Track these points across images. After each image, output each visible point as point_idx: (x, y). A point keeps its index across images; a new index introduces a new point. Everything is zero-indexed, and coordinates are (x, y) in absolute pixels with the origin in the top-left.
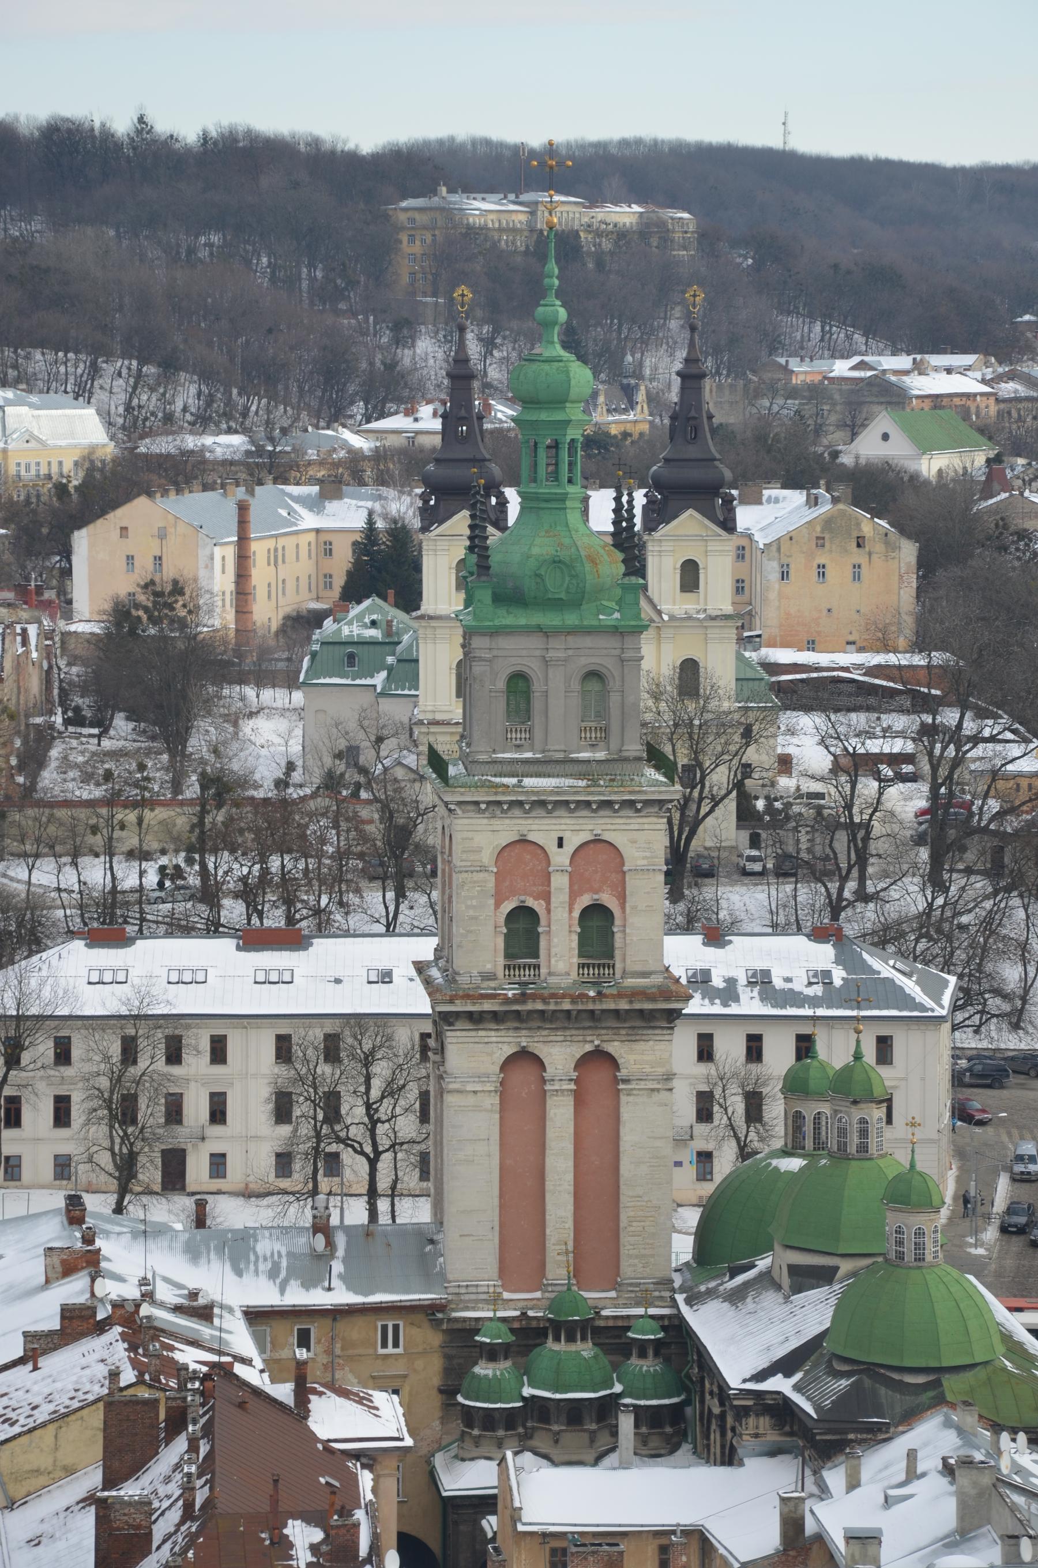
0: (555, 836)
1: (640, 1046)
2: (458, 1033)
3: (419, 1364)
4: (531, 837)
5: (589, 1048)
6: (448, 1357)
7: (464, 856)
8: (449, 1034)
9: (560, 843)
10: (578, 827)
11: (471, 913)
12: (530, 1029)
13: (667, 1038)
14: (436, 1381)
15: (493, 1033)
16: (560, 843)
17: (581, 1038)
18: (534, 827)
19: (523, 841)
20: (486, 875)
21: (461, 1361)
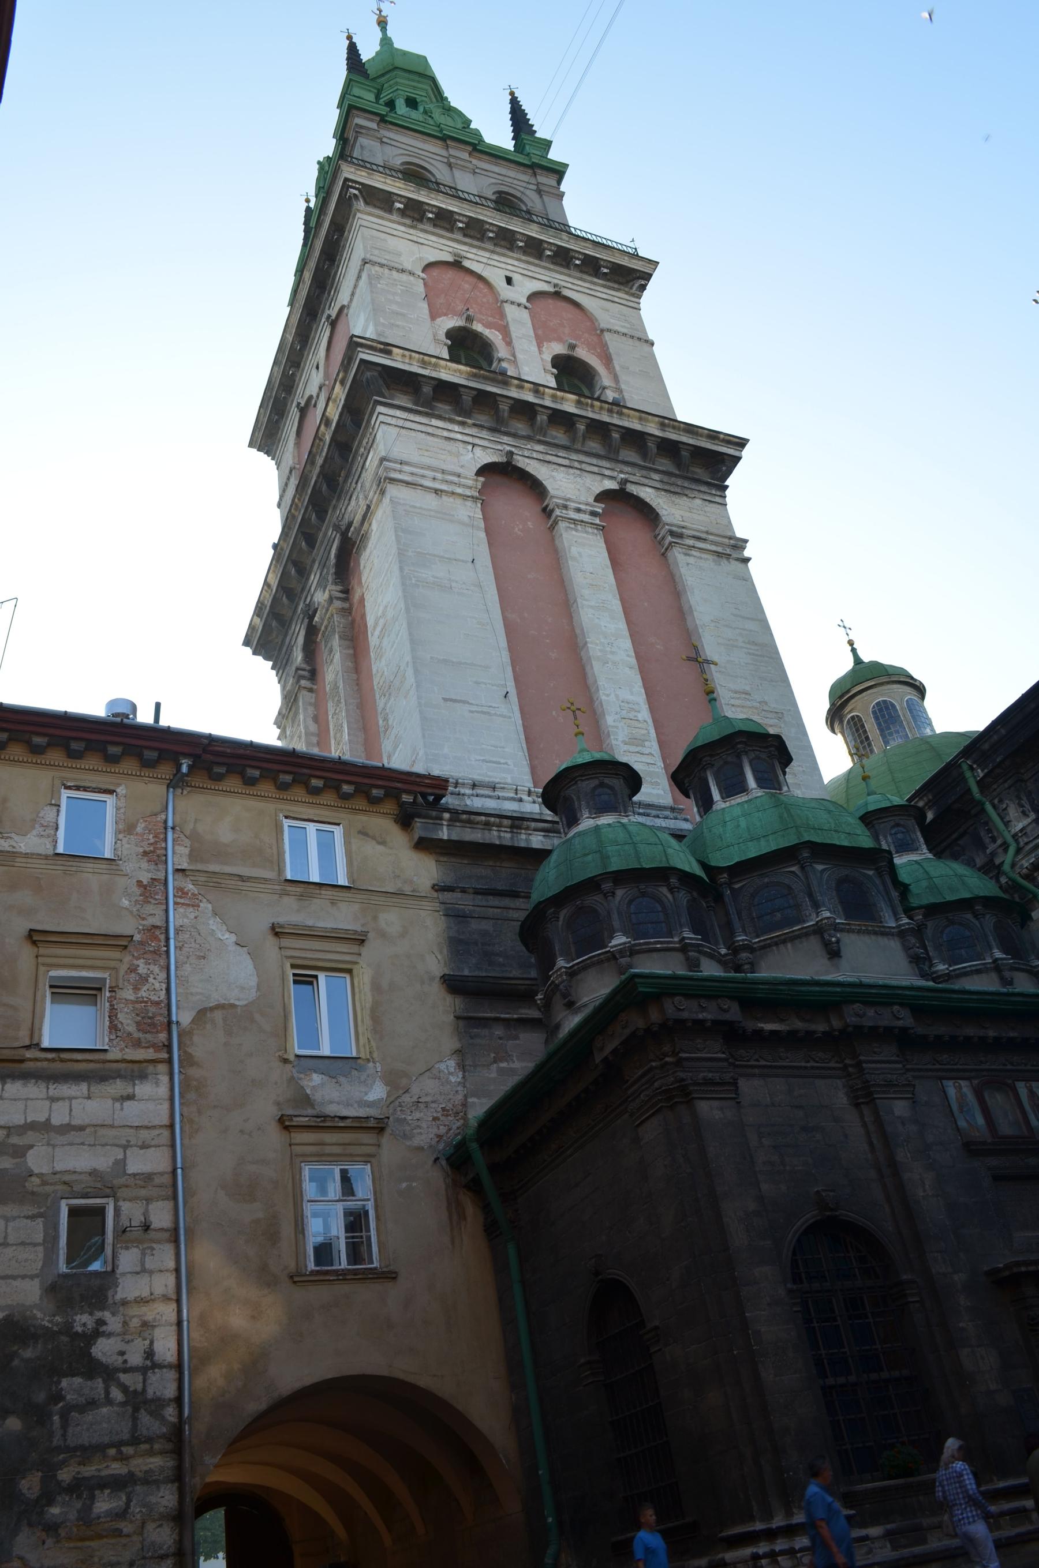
0: (503, 273)
1: (683, 501)
2: (398, 413)
3: (391, 919)
4: (466, 264)
5: (611, 485)
6: (455, 916)
7: (376, 252)
8: (380, 409)
9: (509, 281)
10: (530, 274)
11: (394, 307)
12: (514, 435)
13: (718, 499)
14: (436, 965)
15: (456, 428)
16: (509, 281)
17: (596, 469)
18: (469, 255)
19: (456, 264)
20: (412, 278)
21: (486, 926)
